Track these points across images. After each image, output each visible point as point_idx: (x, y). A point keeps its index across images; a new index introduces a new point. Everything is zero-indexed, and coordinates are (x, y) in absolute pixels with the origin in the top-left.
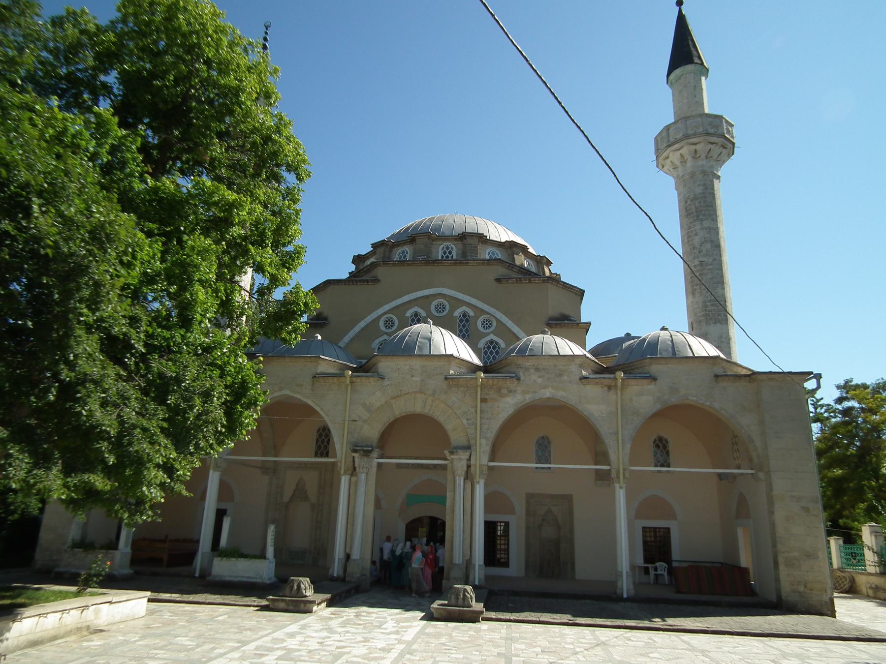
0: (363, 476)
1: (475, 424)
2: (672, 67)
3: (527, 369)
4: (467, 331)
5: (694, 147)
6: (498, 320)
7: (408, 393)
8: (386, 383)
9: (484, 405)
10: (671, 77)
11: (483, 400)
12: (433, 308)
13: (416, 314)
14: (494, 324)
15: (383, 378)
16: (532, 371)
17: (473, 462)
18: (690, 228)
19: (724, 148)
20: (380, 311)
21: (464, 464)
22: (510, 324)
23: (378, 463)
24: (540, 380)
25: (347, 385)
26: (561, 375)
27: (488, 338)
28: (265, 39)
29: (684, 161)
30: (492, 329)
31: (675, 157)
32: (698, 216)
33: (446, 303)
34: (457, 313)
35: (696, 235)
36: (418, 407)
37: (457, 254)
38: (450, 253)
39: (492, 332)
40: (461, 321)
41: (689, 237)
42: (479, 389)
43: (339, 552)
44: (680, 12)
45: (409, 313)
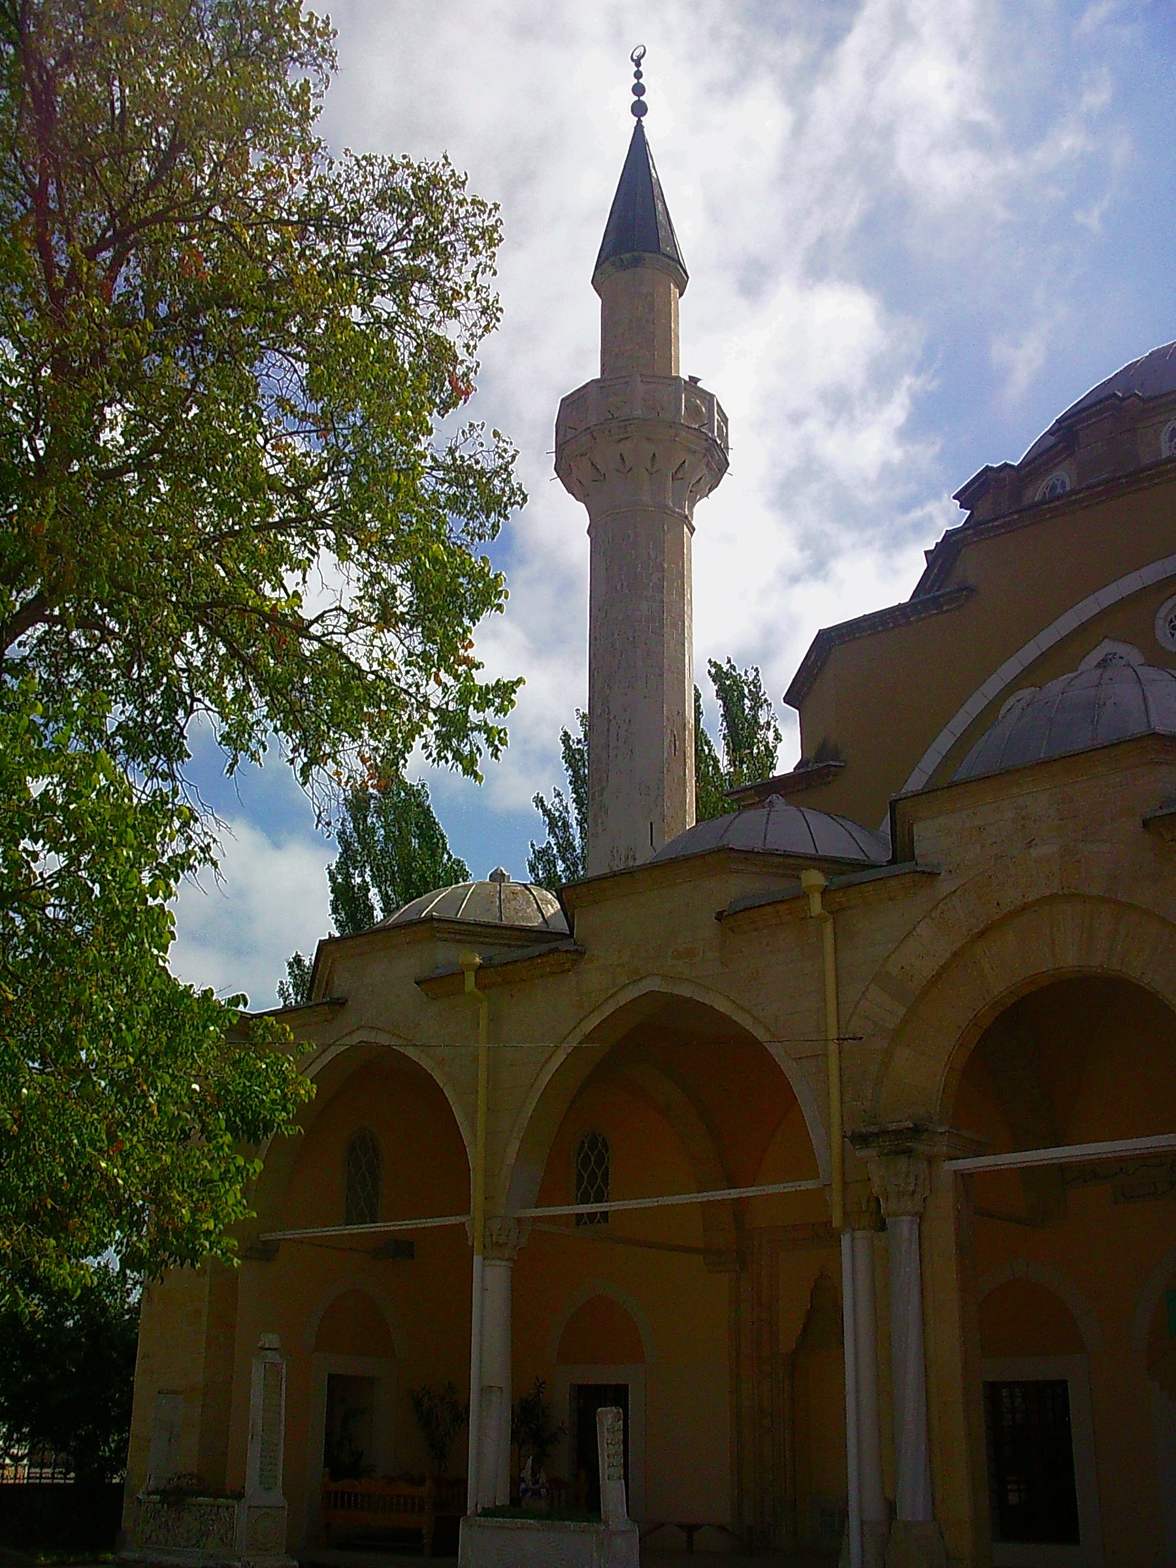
0: (904, 1228)
7: (1024, 909)
8: (944, 887)
15: (932, 875)
23: (963, 1177)
28: (639, 90)
36: (1064, 949)
43: (861, 1498)
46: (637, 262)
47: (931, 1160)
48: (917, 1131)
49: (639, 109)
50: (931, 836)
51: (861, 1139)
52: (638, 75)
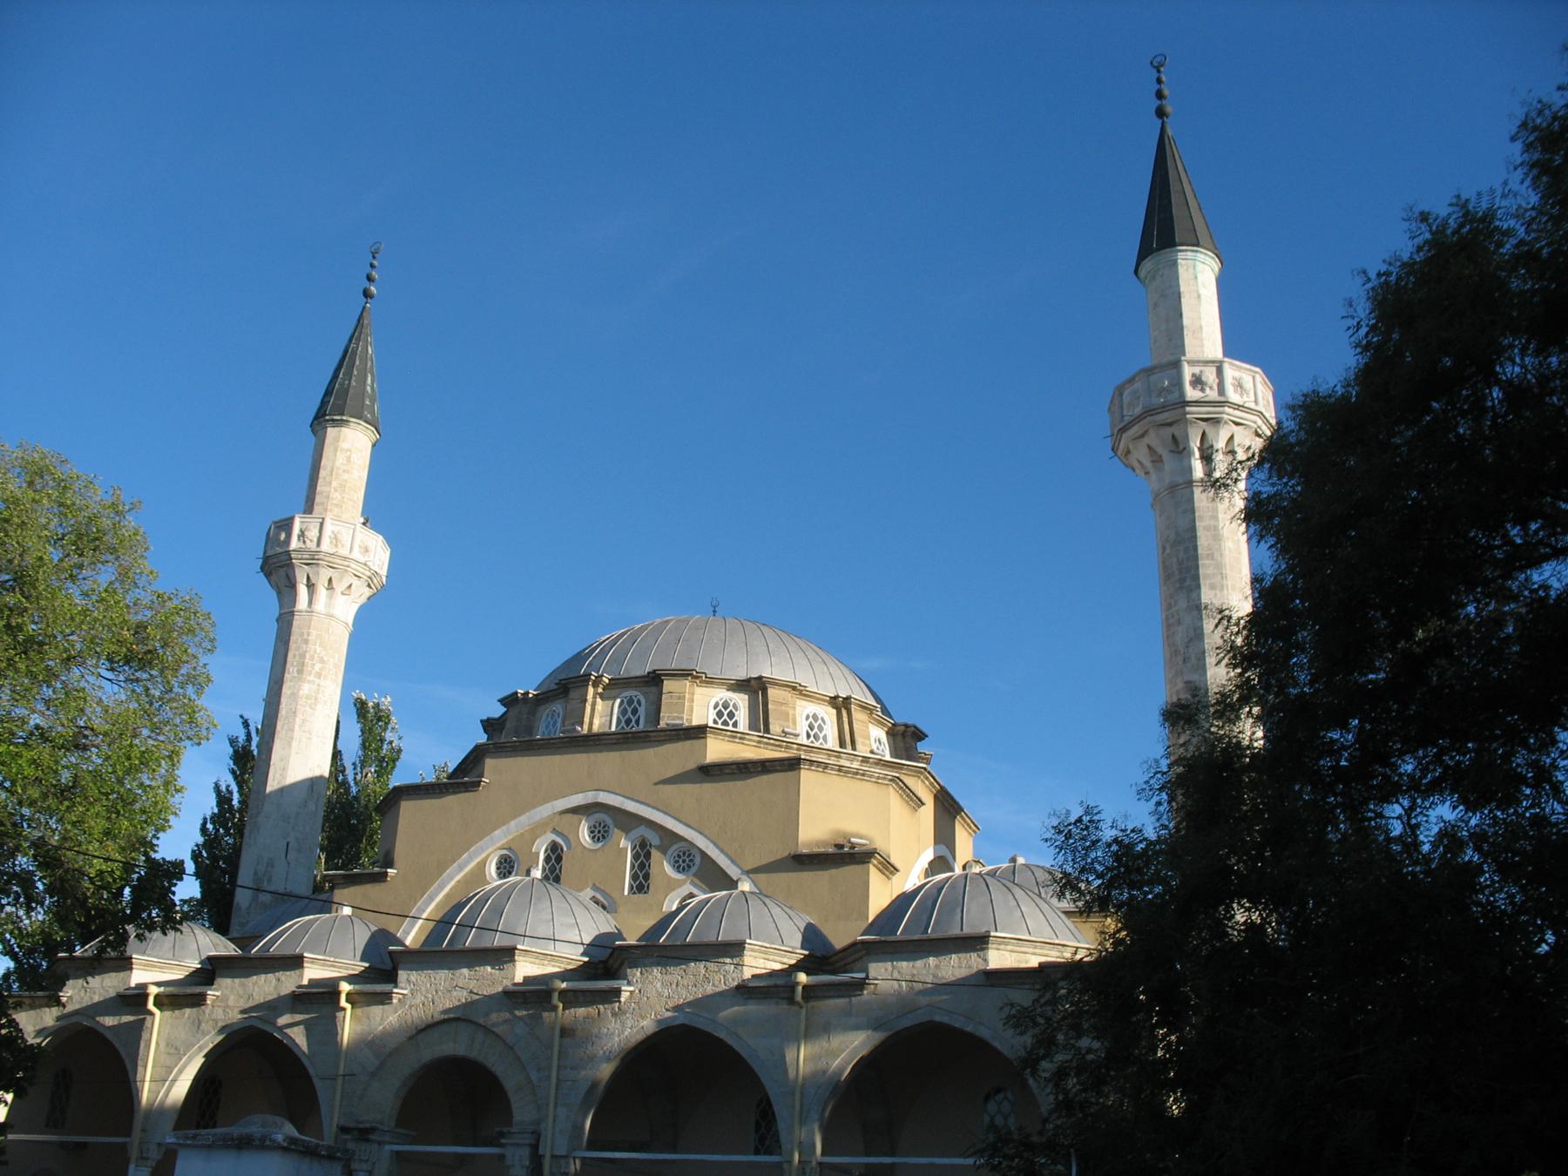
1: (549, 1077)
2: (1145, 252)
4: (647, 877)
5: (1169, 431)
6: (703, 854)
10: (1142, 274)
14: (698, 860)
18: (1169, 607)
19: (1237, 424)
21: (526, 1152)
22: (723, 861)
28: (370, 279)
29: (1157, 460)
30: (694, 869)
31: (1140, 454)
32: (1182, 581)
33: (609, 821)
35: (1179, 622)
37: (646, 715)
38: (635, 711)
41: (1169, 626)
44: (1163, 129)
47: (380, 1143)
48: (373, 1130)
51: (344, 1130)
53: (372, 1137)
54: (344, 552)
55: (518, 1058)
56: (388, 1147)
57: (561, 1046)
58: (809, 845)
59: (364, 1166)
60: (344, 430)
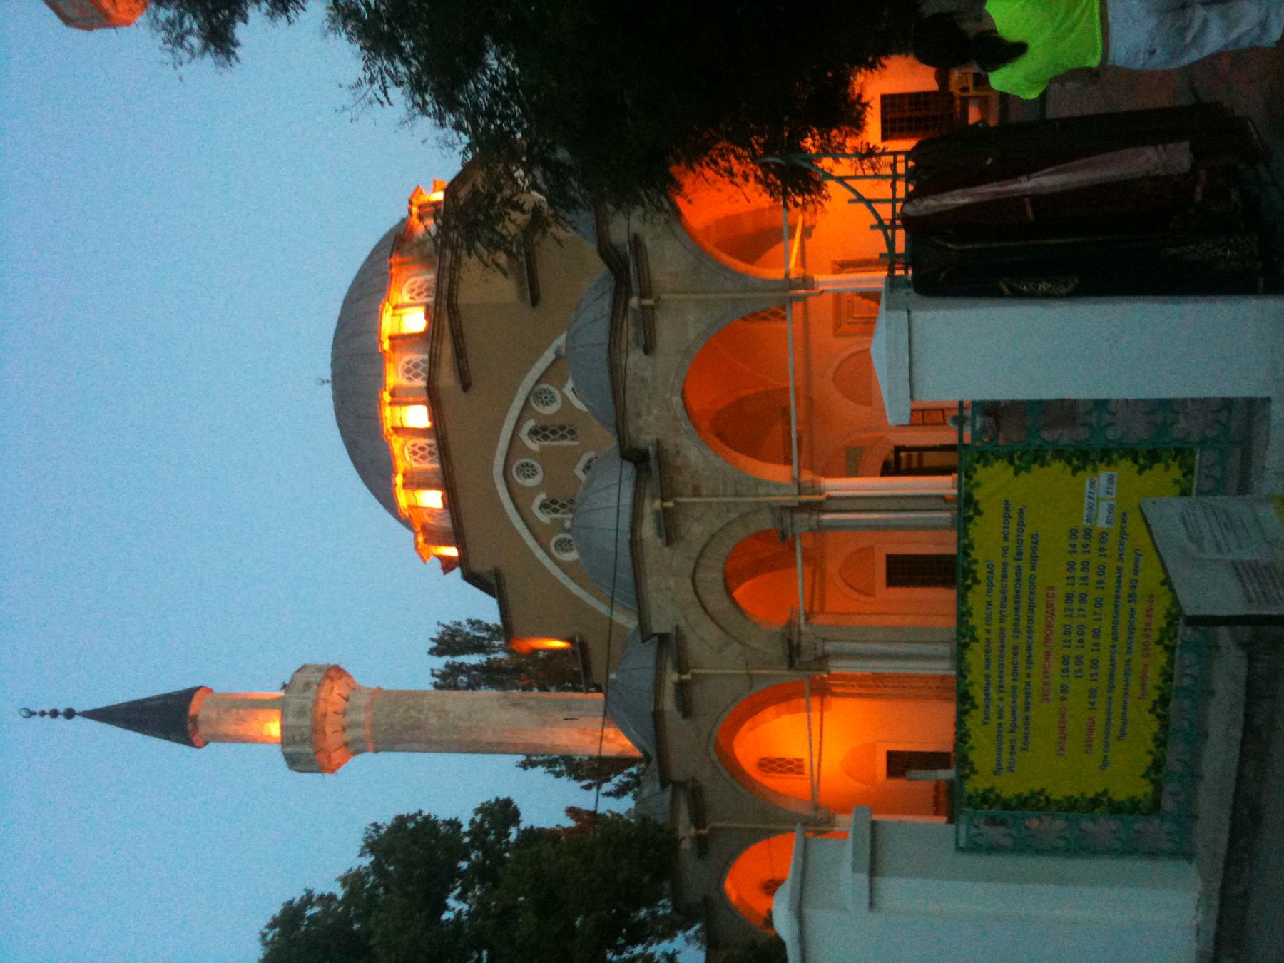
3: (639, 430)
4: (563, 428)
6: (538, 382)
7: (696, 592)
8: (682, 622)
9: (704, 491)
11: (697, 492)
12: (530, 482)
13: (544, 506)
14: (544, 386)
16: (641, 423)
17: (795, 504)
20: (547, 563)
21: (797, 517)
24: (655, 412)
25: (693, 675)
26: (643, 380)
27: (571, 396)
28: (54, 714)
30: (552, 389)
34: (534, 446)
38: (422, 449)
39: (560, 390)
40: (546, 438)
42: (678, 499)
45: (544, 518)
46: (194, 720)
47: (800, 633)
48: (790, 642)
49: (70, 714)
50: (660, 625)
52: (43, 714)
53: (795, 643)
54: (310, 705)
55: (721, 530)
56: (803, 628)
57: (708, 496)
58: (521, 295)
59: (820, 645)
60: (200, 718)
